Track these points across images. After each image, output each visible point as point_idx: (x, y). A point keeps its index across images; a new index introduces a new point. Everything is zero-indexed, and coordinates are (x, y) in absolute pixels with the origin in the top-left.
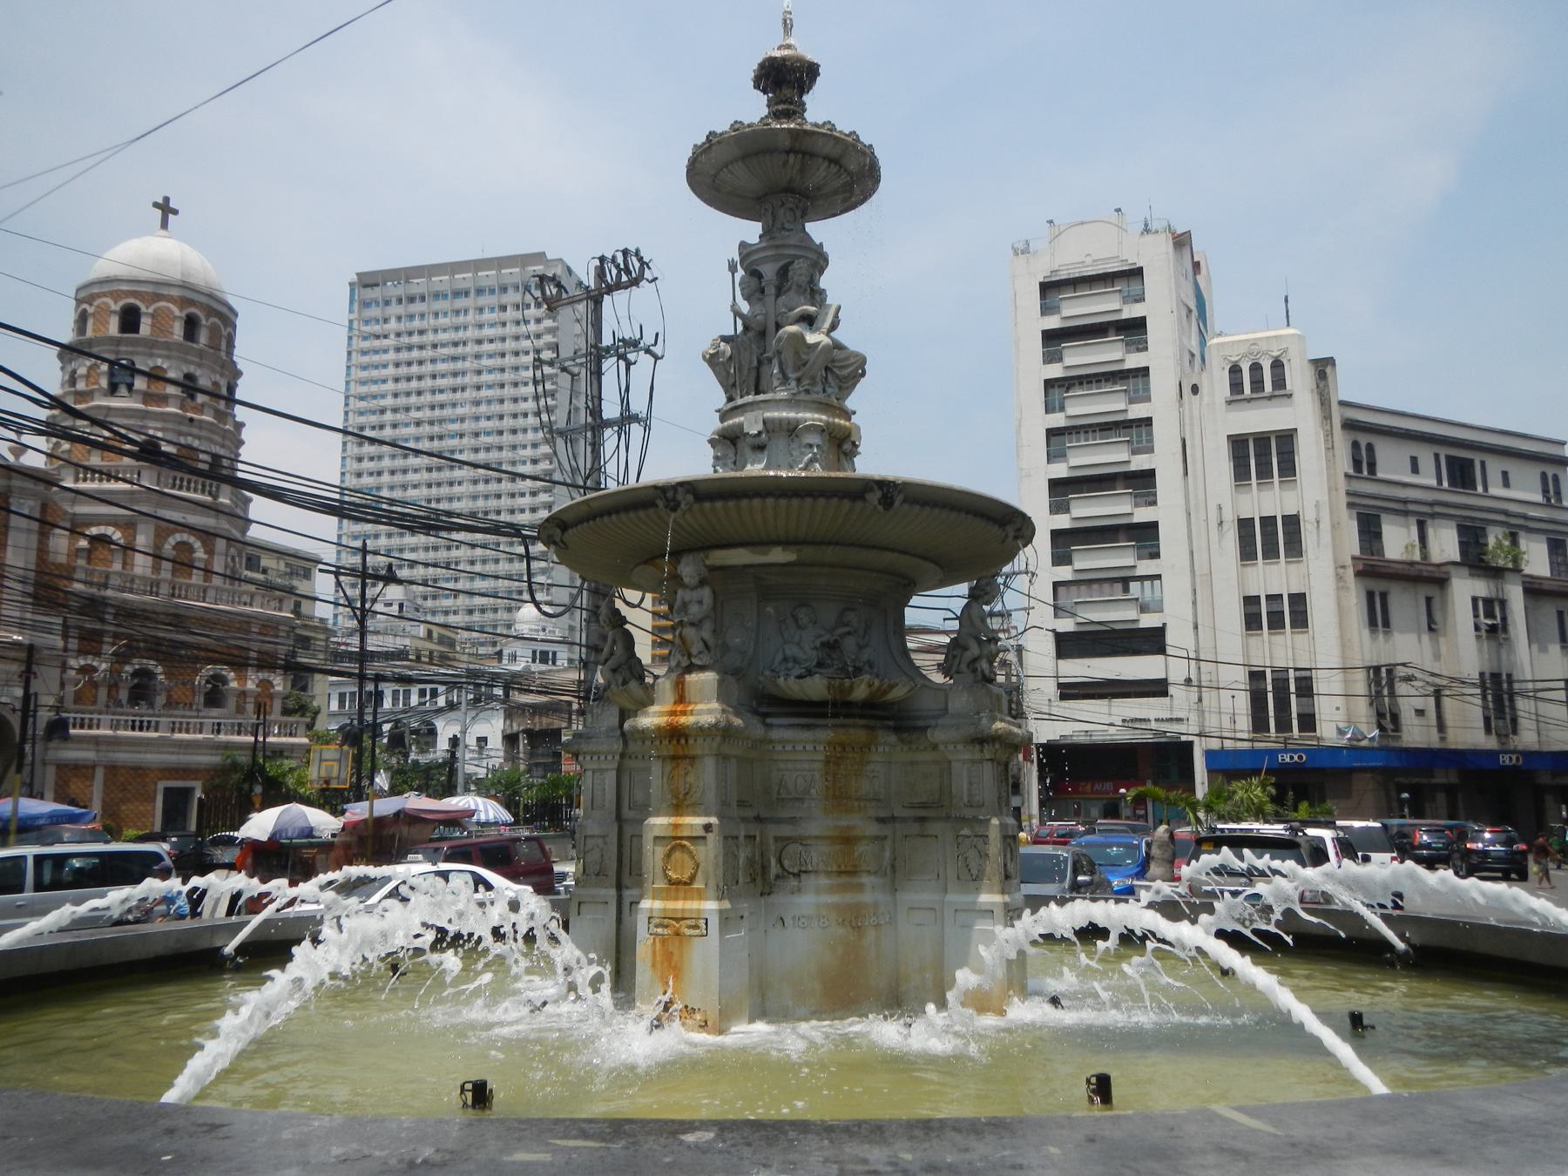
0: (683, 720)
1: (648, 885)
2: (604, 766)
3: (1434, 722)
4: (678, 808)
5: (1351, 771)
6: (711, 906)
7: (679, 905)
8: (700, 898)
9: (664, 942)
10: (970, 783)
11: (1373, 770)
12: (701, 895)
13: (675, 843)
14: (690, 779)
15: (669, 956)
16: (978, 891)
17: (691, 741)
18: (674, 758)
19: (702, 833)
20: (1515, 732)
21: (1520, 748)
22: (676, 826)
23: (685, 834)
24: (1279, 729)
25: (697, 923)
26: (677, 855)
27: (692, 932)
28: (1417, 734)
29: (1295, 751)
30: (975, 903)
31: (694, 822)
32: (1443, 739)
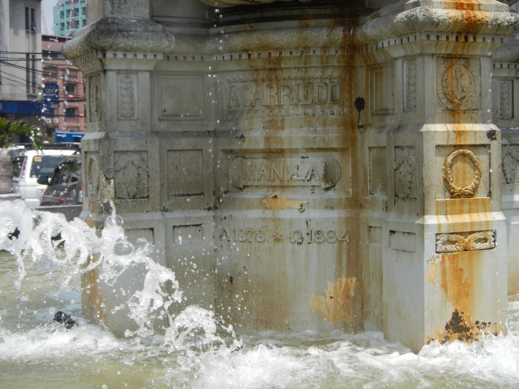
0: (479, 15)
2: (134, 67)
4: (454, 112)
6: (497, 216)
7: (466, 218)
8: (485, 210)
9: (454, 258)
10: (502, 99)
13: (461, 151)
14: (465, 82)
17: (479, 40)
18: (449, 58)
19: (486, 141)
22: (459, 134)
23: (470, 142)
25: (486, 236)
26: (459, 165)
27: (479, 246)
30: (512, 202)
31: (477, 129)
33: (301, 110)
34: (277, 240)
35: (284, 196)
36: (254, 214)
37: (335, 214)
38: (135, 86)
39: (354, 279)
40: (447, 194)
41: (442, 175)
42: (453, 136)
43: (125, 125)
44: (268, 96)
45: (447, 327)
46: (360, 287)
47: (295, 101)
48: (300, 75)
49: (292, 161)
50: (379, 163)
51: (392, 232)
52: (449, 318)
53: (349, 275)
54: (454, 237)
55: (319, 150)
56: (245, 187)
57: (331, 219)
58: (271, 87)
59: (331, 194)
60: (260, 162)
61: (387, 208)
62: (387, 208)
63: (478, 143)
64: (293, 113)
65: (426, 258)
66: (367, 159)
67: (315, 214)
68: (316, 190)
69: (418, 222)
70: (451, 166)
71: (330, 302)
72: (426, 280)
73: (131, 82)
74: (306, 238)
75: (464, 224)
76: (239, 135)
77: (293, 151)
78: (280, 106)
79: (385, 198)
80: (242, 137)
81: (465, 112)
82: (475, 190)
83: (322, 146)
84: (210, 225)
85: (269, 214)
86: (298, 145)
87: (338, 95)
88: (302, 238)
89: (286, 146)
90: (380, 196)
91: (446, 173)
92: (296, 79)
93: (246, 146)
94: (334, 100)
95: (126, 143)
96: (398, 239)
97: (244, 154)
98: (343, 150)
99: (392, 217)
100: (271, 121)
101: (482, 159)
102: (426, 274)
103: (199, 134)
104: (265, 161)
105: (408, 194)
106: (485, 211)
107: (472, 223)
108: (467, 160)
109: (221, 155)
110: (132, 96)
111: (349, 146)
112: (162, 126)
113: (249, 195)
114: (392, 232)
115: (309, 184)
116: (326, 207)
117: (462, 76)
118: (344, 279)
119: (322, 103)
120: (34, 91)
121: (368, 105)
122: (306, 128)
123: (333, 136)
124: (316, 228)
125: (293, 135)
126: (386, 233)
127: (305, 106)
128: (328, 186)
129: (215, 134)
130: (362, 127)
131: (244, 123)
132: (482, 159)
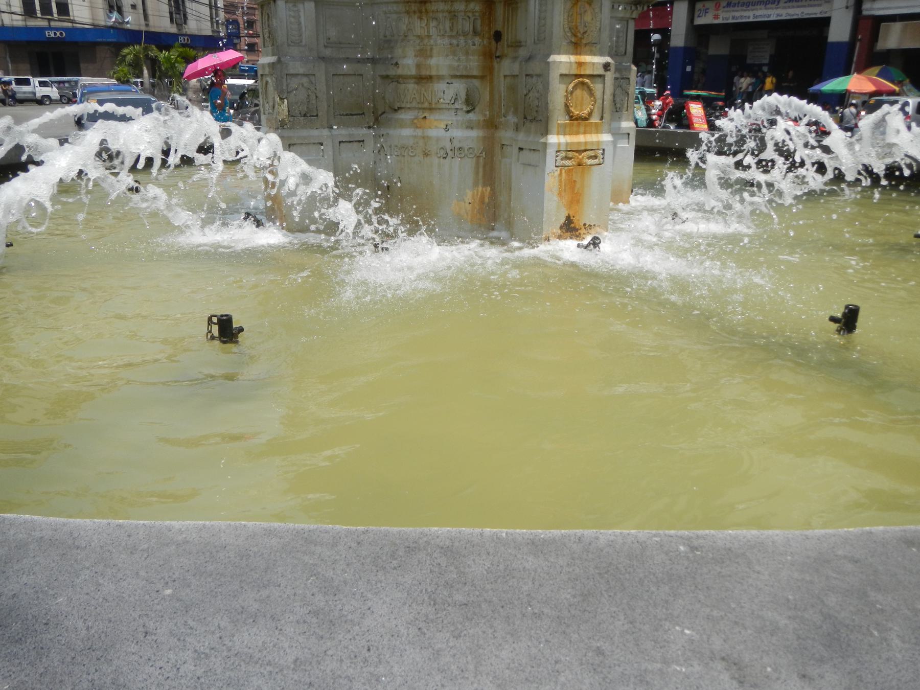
1: (553, 126)
3: (142, 11)
4: (577, 45)
5: (95, 44)
6: (606, 137)
7: (581, 138)
9: (570, 172)
11: (108, 44)
12: (597, 129)
13: (581, 80)
14: (588, 18)
15: (572, 184)
16: (620, 119)
19: (601, 71)
20: (185, 23)
21: (188, 33)
22: (580, 64)
23: (588, 72)
24: (59, 13)
25: (597, 154)
26: (578, 92)
27: (590, 162)
28: (132, 20)
29: (57, 29)
30: (620, 128)
31: (595, 61)
32: (147, 25)
33: (447, 41)
34: (426, 154)
35: (432, 117)
36: (406, 132)
37: (474, 133)
38: (302, 14)
39: (489, 189)
40: (567, 117)
41: (563, 100)
42: (574, 66)
43: (295, 51)
44: (419, 27)
45: (561, 228)
46: (493, 194)
47: (442, 32)
48: (446, 8)
49: (440, 86)
50: (512, 89)
51: (521, 149)
52: (563, 220)
53: (484, 185)
54: (570, 154)
55: (461, 77)
56: (399, 108)
57: (470, 137)
58: (421, 18)
59: (471, 116)
60: (411, 86)
61: (517, 129)
62: (517, 129)
63: (595, 73)
64: (440, 42)
65: (547, 171)
66: (502, 85)
67: (458, 133)
68: (459, 113)
69: (542, 140)
70: (572, 93)
71: (469, 207)
72: (546, 188)
73: (298, 11)
74: (450, 153)
75: (579, 143)
76: (394, 62)
77: (440, 78)
78: (429, 37)
79: (515, 120)
80: (397, 64)
81: (586, 44)
82: (590, 114)
83: (464, 73)
84: (370, 143)
85: (419, 132)
86: (444, 72)
87: (479, 28)
88: (447, 154)
89: (434, 73)
90: (512, 119)
91: (567, 99)
92: (443, 11)
93: (400, 72)
94: (475, 33)
95: (297, 67)
96: (526, 156)
97: (398, 79)
98: (482, 78)
99: (521, 136)
100: (421, 50)
101: (597, 87)
102: (546, 184)
103: (359, 61)
104: (416, 86)
105: (535, 117)
106: (597, 133)
107: (586, 143)
108: (585, 88)
109: (379, 80)
110: (300, 24)
111: (487, 74)
112: (328, 52)
113: (405, 116)
114: (521, 149)
115: (453, 107)
116: (467, 127)
117: (585, 12)
118: (480, 189)
119: (465, 34)
120: (218, 27)
121: (504, 37)
122: (451, 57)
123: (474, 64)
124: (457, 144)
125: (439, 63)
126: (516, 150)
127: (451, 37)
128: (469, 109)
129: (373, 61)
130: (498, 57)
131: (398, 52)
132: (597, 87)
